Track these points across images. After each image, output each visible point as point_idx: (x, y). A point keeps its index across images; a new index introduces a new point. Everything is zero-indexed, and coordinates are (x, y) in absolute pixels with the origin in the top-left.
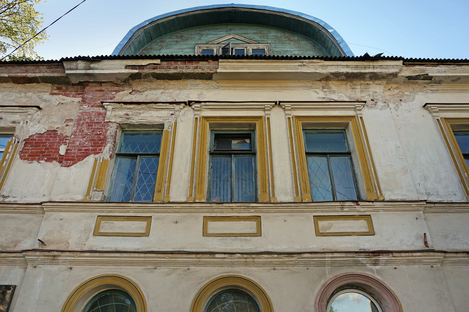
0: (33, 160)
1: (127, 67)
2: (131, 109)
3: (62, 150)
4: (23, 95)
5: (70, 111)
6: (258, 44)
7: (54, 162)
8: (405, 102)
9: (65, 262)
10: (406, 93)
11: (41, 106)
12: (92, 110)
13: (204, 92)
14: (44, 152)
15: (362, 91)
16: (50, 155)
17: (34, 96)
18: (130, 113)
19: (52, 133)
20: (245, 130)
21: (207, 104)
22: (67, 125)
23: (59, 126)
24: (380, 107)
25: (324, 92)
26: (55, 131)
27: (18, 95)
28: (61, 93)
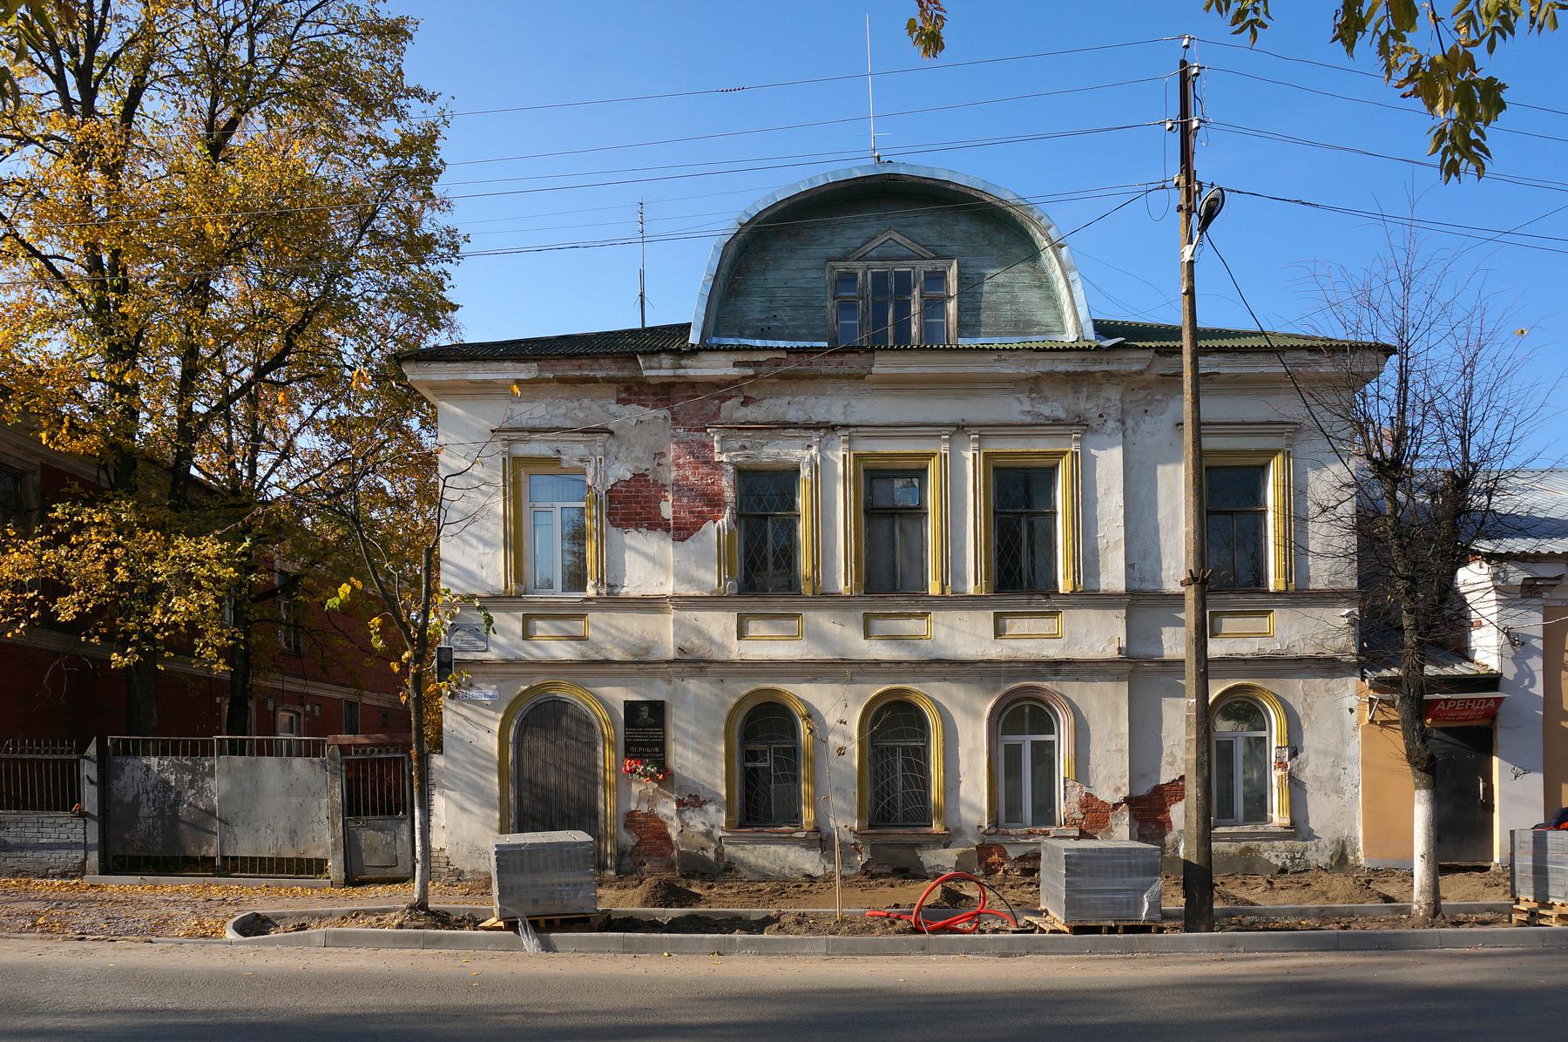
0: (628, 526)
1: (735, 365)
2: (748, 437)
3: (667, 510)
4: (576, 404)
5: (656, 437)
6: (934, 259)
7: (659, 530)
9: (714, 673)
10: (1158, 397)
11: (611, 427)
12: (691, 438)
13: (853, 402)
14: (641, 514)
15: (1088, 398)
16: (650, 519)
17: (594, 406)
18: (747, 444)
19: (639, 477)
20: (913, 464)
21: (859, 429)
22: (659, 465)
23: (648, 466)
24: (1109, 431)
25: (1032, 399)
26: (644, 475)
27: (570, 405)
28: (632, 398)
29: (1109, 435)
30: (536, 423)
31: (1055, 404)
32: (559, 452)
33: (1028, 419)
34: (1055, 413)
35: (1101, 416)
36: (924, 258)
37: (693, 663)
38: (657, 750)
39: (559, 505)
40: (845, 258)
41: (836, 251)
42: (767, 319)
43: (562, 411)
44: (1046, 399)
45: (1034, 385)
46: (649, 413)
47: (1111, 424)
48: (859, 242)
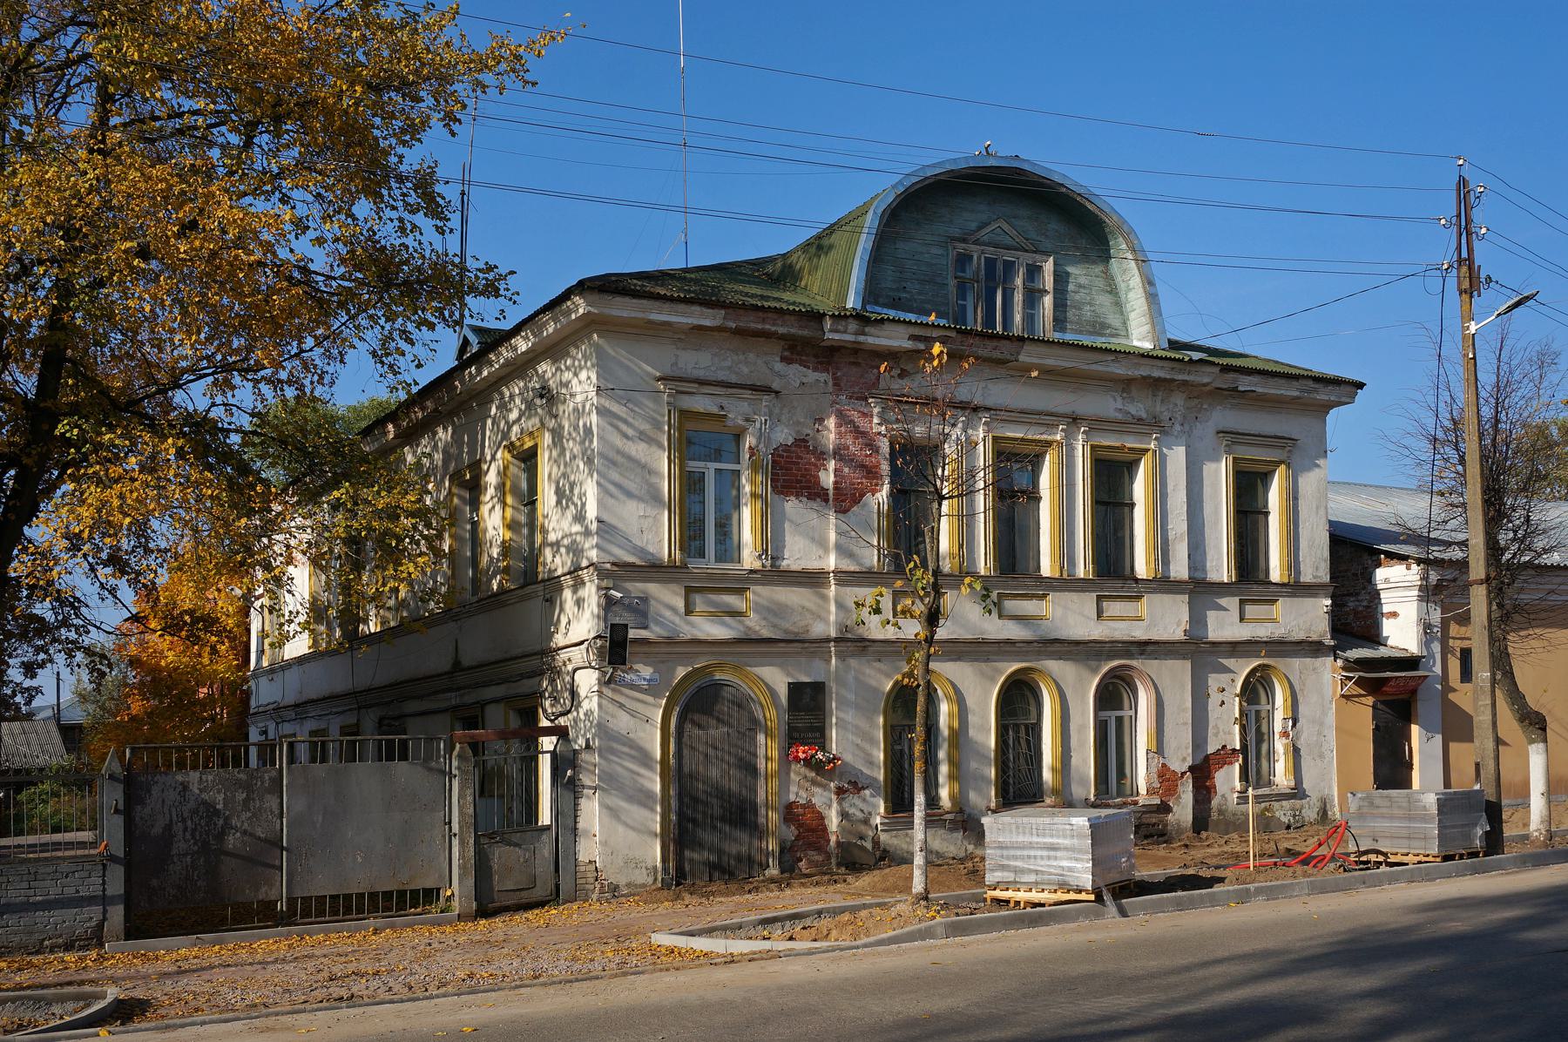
3: (828, 479)
7: (819, 500)
8: (1200, 422)
10: (1205, 406)
11: (775, 386)
15: (1162, 401)
16: (809, 488)
17: (759, 362)
19: (801, 442)
25: (1124, 399)
27: (735, 358)
28: (794, 357)
29: (1176, 437)
30: (701, 374)
31: (1139, 405)
32: (722, 408)
33: (1119, 416)
34: (1140, 413)
35: (1170, 419)
36: (1026, 251)
37: (853, 644)
38: (818, 735)
39: (713, 466)
40: (964, 241)
41: (956, 232)
42: (898, 290)
43: (728, 363)
44: (1132, 400)
45: (1126, 385)
46: (812, 376)
47: (1178, 427)
48: (974, 225)
